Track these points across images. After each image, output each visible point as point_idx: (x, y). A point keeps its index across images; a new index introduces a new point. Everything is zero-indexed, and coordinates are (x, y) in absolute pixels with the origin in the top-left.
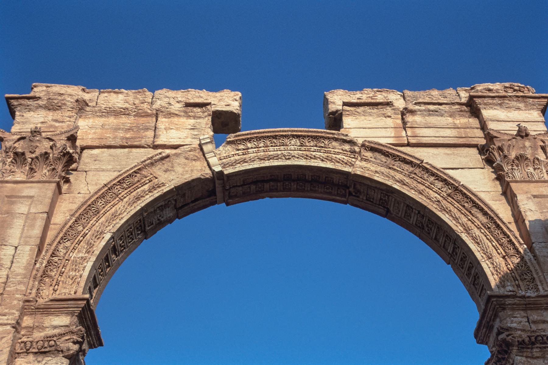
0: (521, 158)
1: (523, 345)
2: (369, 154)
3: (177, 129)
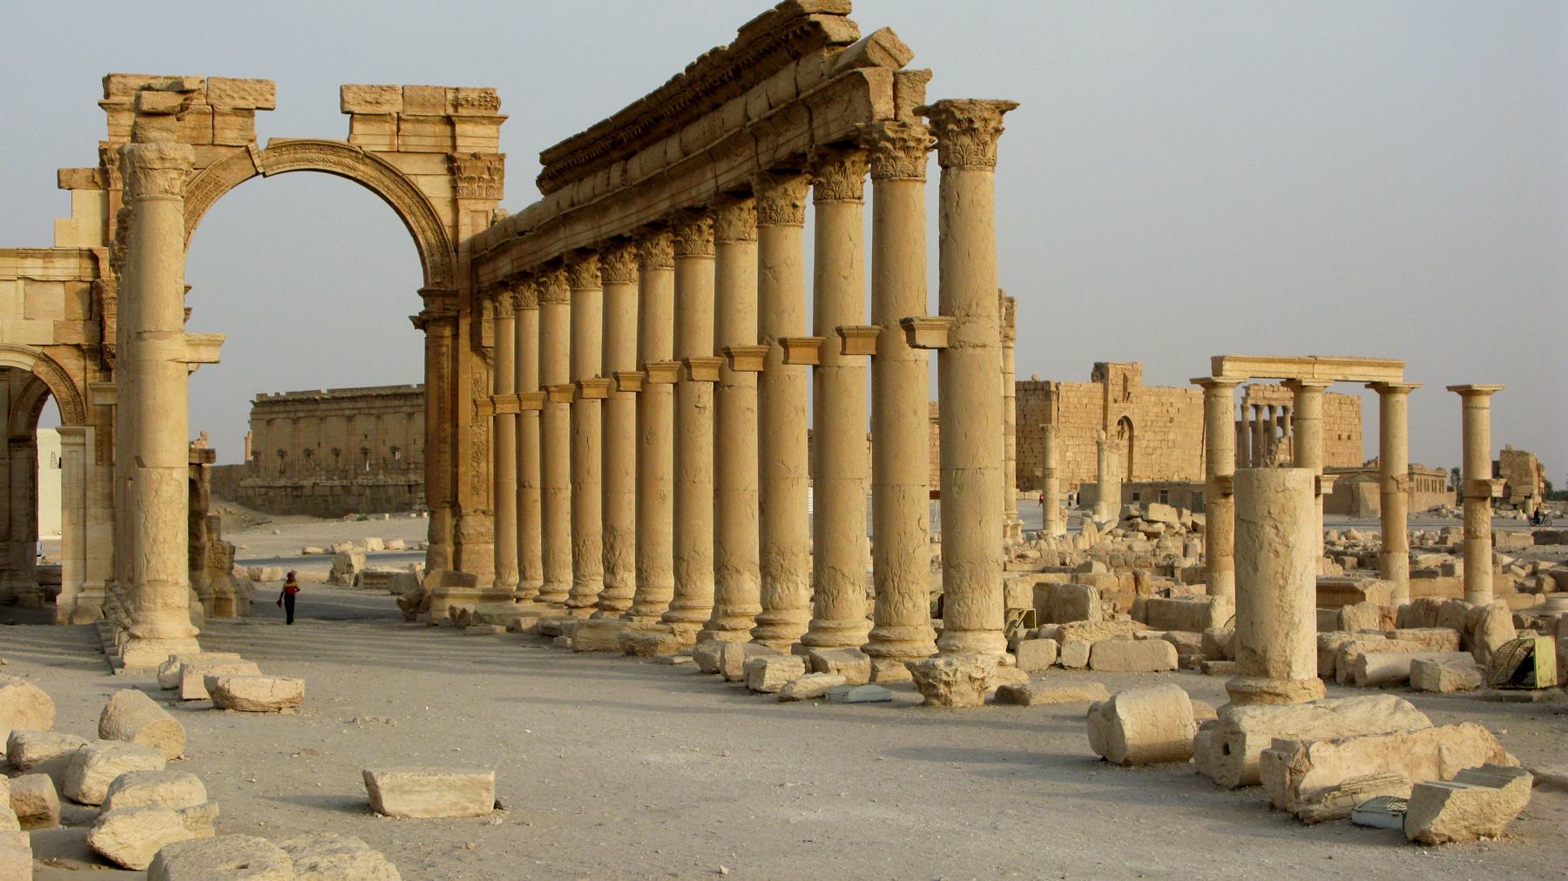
0: (471, 179)
1: (435, 319)
2: (368, 161)
3: (229, 129)
